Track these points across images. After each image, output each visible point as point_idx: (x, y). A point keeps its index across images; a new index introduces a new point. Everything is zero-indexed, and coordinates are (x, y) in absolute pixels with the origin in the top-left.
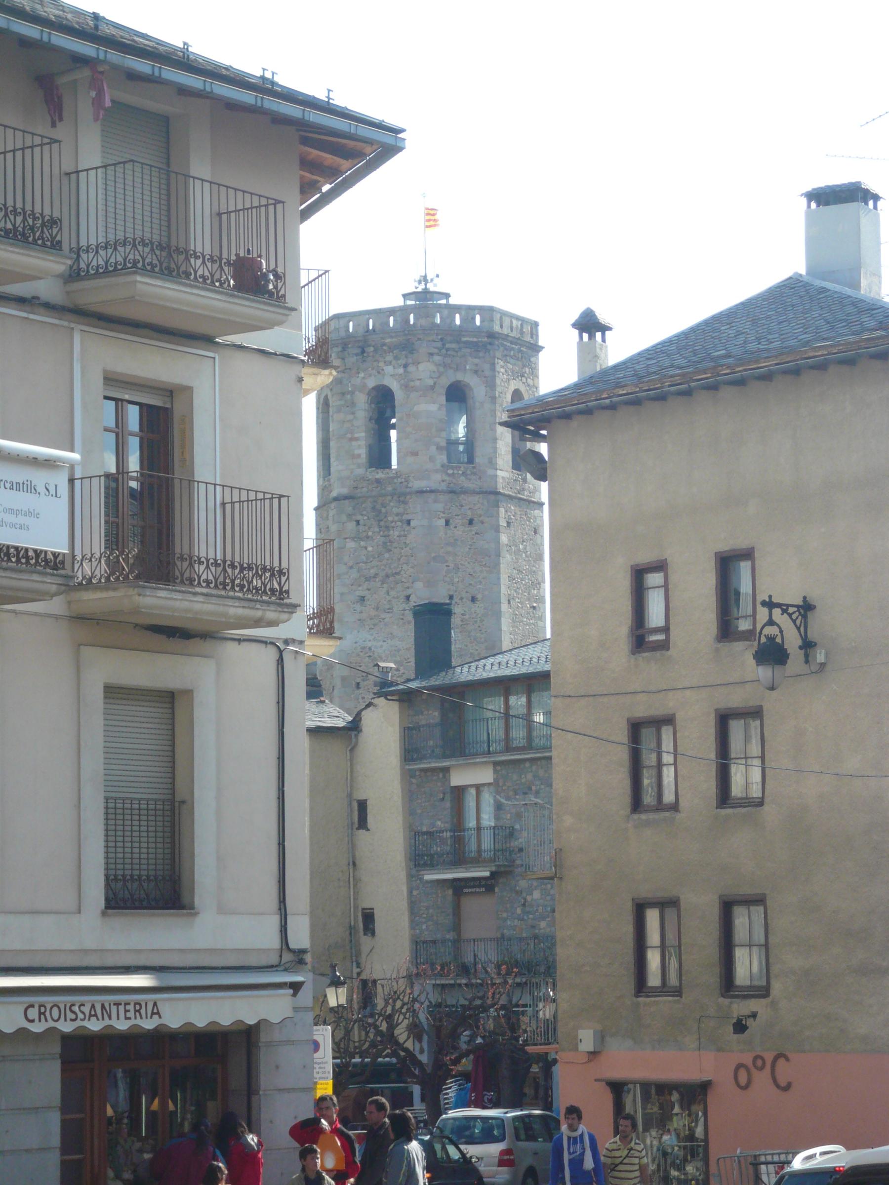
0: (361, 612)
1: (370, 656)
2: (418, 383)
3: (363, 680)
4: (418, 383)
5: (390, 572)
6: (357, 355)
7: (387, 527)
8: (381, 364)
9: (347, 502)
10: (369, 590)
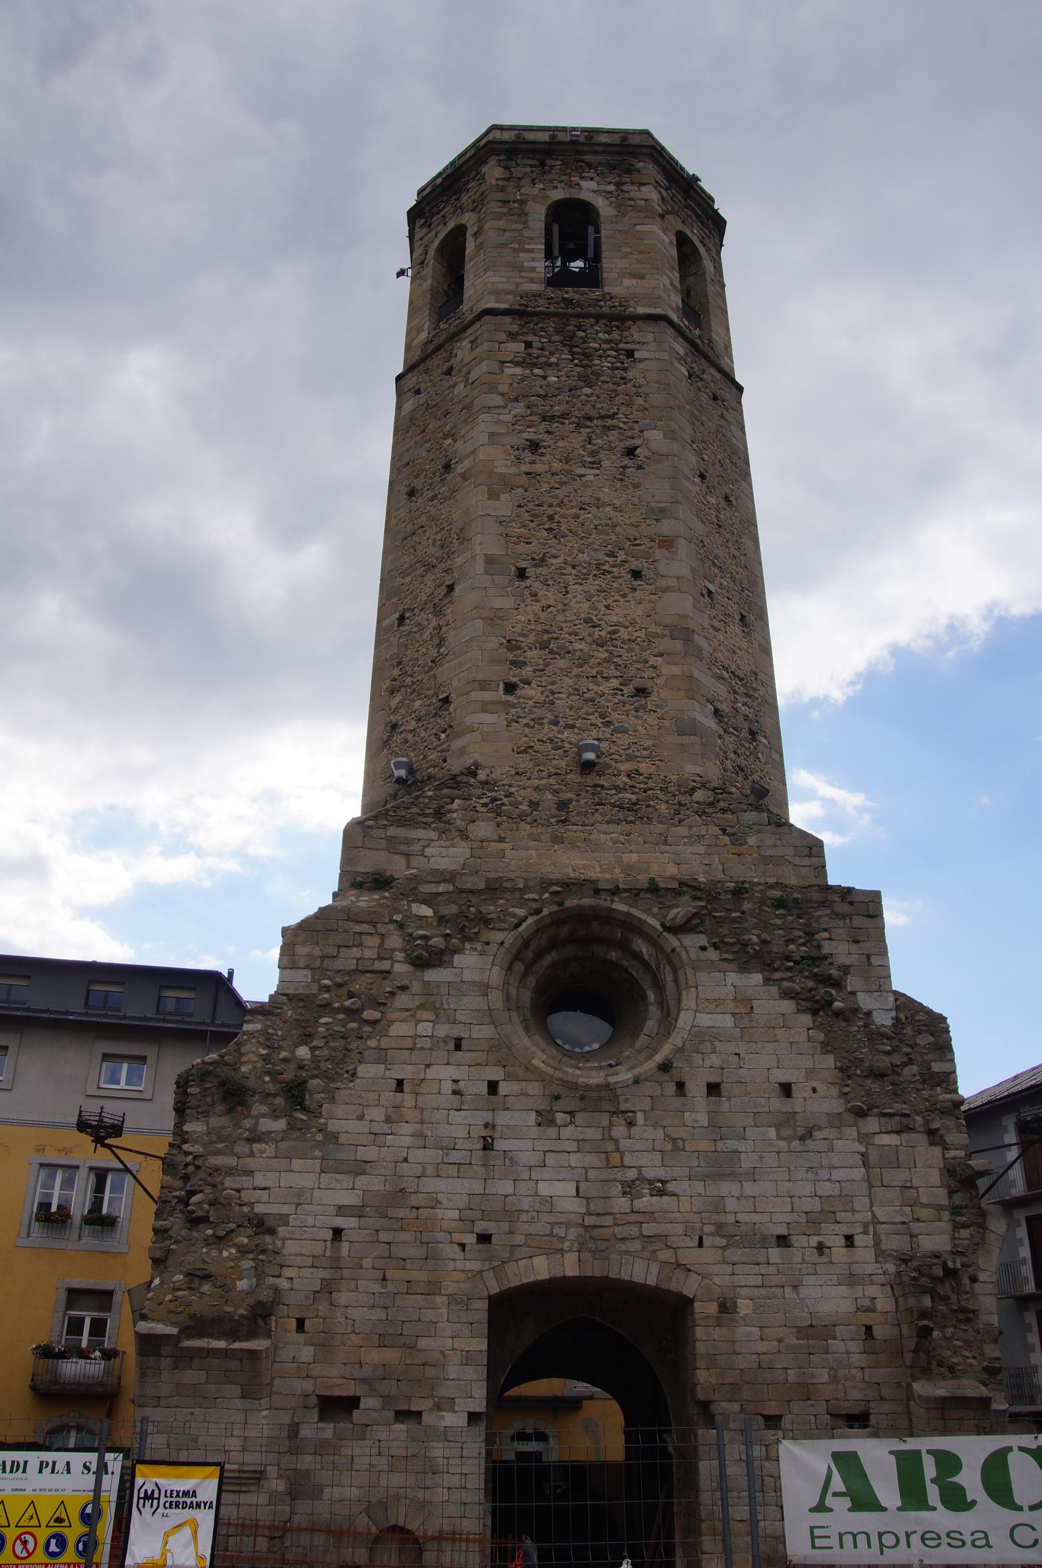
0: (533, 462)
1: (550, 529)
2: (642, 203)
3: (535, 566)
4: (642, 203)
5: (593, 413)
6: (531, 166)
7: (587, 356)
8: (576, 179)
9: (508, 319)
10: (549, 433)
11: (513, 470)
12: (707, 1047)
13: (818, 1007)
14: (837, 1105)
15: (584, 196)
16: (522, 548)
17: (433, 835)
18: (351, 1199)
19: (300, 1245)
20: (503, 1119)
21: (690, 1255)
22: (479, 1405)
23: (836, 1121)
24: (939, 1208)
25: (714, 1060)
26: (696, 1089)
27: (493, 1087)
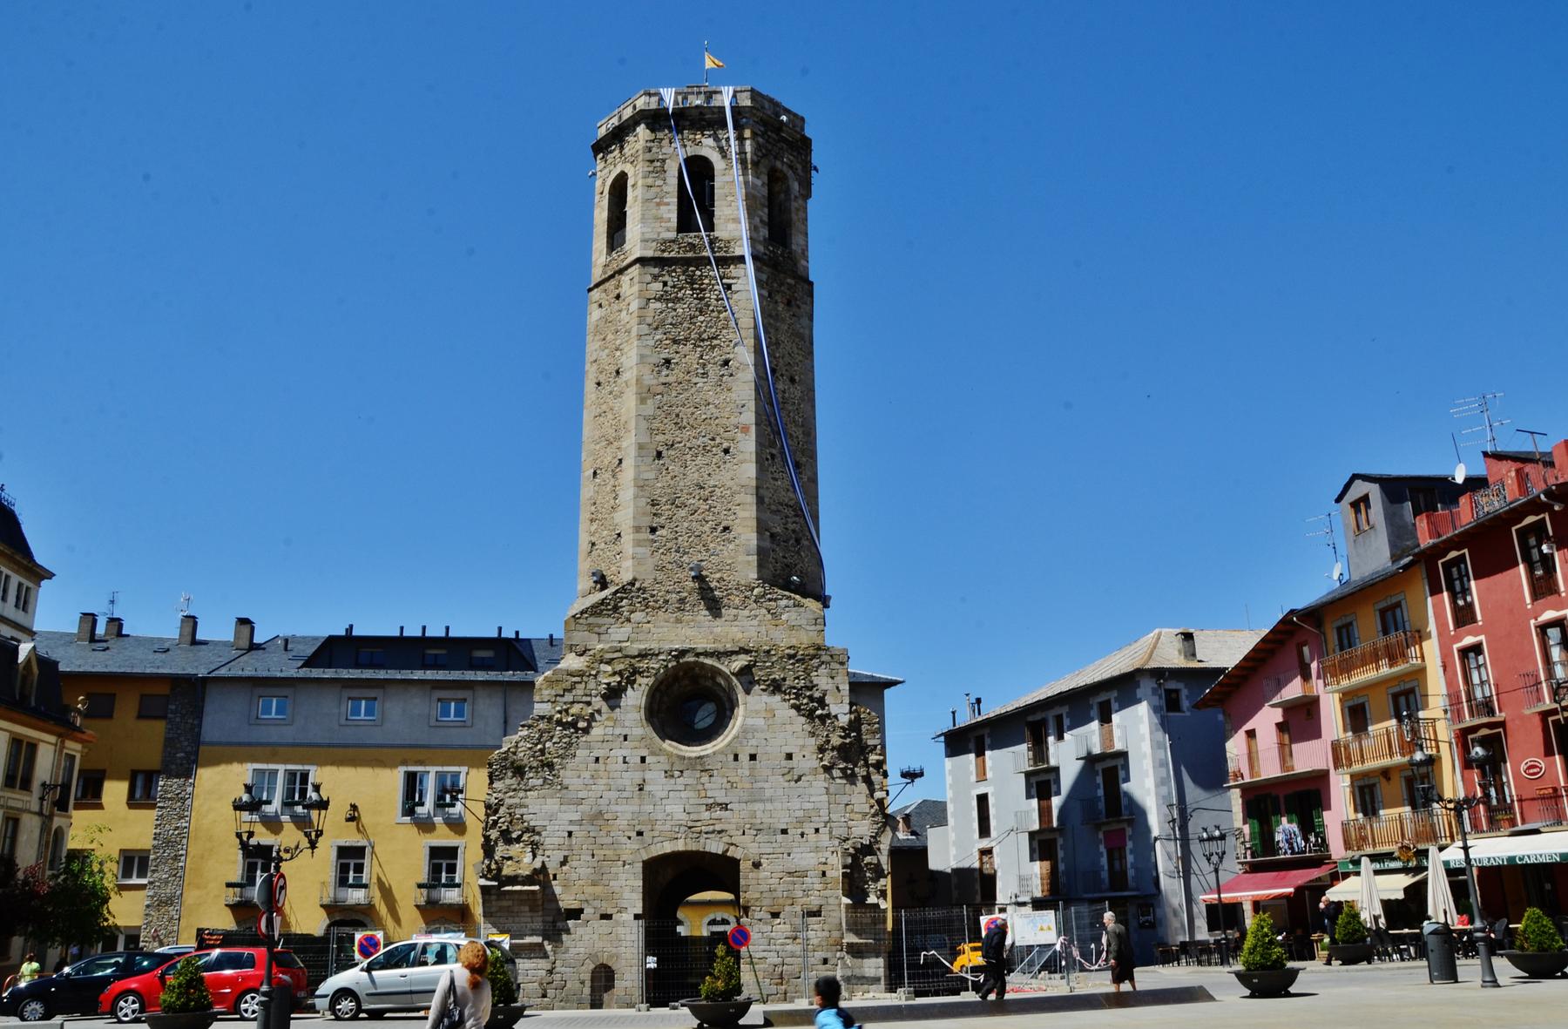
11: (655, 382)
12: (750, 735)
13: (810, 715)
14: (816, 764)
15: (705, 152)
16: (660, 438)
17: (611, 620)
18: (576, 817)
19: (552, 838)
20: (648, 775)
21: (737, 839)
22: (639, 911)
23: (814, 771)
24: (865, 814)
25: (753, 742)
26: (744, 758)
27: (643, 760)
